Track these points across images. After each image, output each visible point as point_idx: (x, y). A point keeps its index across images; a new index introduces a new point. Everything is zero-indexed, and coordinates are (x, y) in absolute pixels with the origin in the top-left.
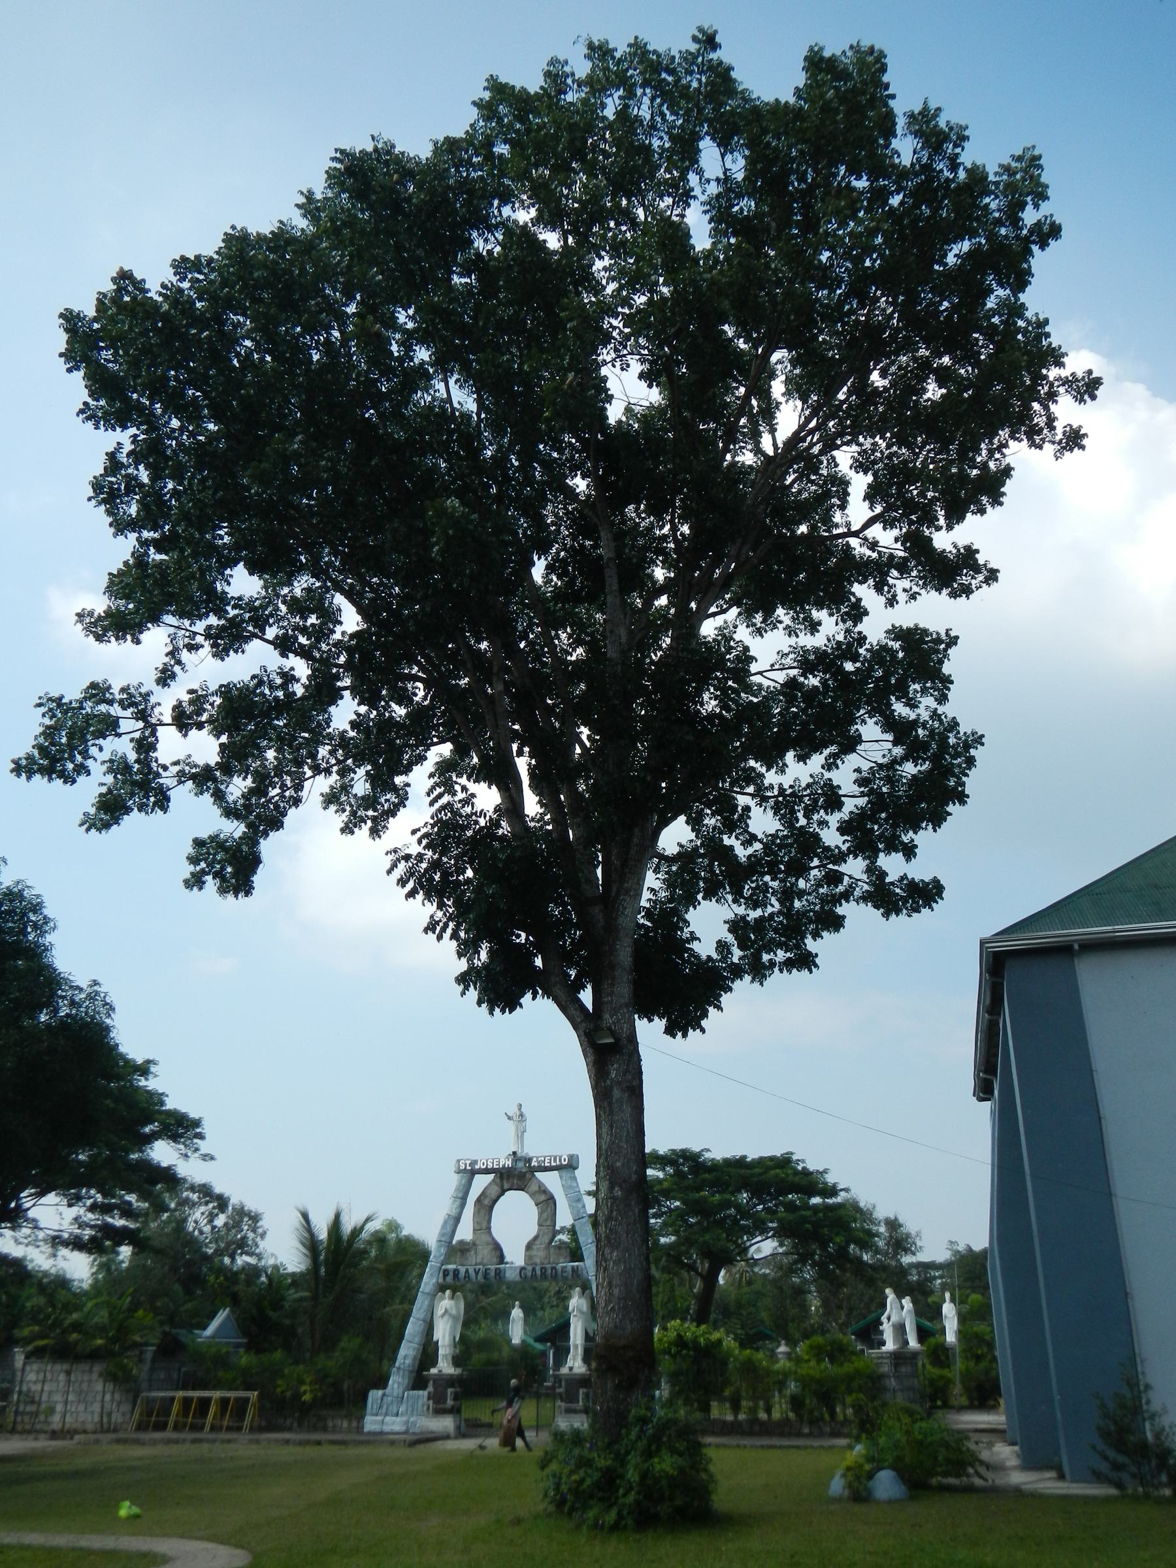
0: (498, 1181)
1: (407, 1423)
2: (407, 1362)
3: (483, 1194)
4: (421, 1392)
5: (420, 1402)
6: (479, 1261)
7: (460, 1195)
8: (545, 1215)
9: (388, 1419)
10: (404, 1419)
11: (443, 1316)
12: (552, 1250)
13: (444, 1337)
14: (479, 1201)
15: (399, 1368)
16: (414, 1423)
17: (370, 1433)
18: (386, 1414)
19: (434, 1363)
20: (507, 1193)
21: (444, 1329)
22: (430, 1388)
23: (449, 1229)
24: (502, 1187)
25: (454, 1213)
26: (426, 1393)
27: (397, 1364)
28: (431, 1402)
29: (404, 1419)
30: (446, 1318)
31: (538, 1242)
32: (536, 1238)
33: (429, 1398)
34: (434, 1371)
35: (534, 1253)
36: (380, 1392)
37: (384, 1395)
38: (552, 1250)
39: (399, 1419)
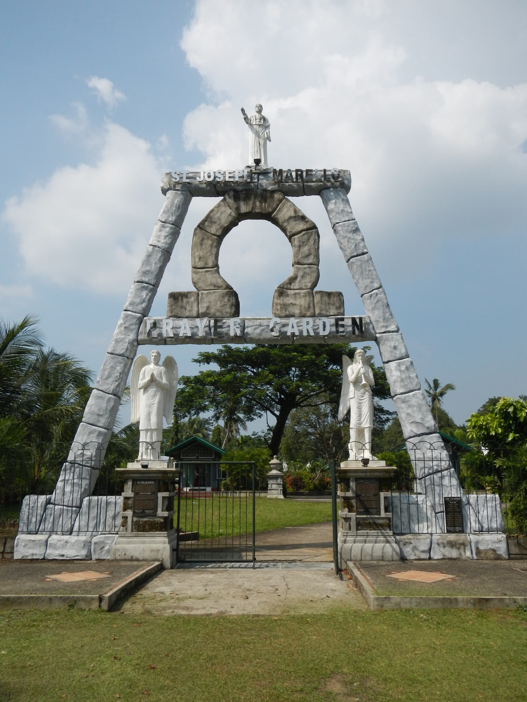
0: (231, 201)
1: (87, 544)
2: (88, 453)
3: (208, 218)
4: (112, 499)
5: (111, 513)
6: (202, 310)
7: (172, 219)
8: (305, 250)
9: (54, 537)
10: (83, 538)
11: (146, 388)
12: (317, 298)
13: (149, 414)
14: (201, 227)
15: (73, 463)
16: (101, 545)
17: (23, 560)
18: (52, 531)
19: (132, 456)
20: (245, 225)
21: (150, 406)
22: (128, 492)
23: (154, 267)
24: (238, 209)
25: (163, 242)
26: (120, 500)
27: (71, 457)
28: (129, 513)
29: (83, 538)
30: (152, 391)
31: (296, 285)
32: (292, 280)
33: (125, 508)
34: (133, 466)
35: (289, 300)
36: (42, 498)
37: (48, 502)
38: (317, 298)
39: (73, 538)
